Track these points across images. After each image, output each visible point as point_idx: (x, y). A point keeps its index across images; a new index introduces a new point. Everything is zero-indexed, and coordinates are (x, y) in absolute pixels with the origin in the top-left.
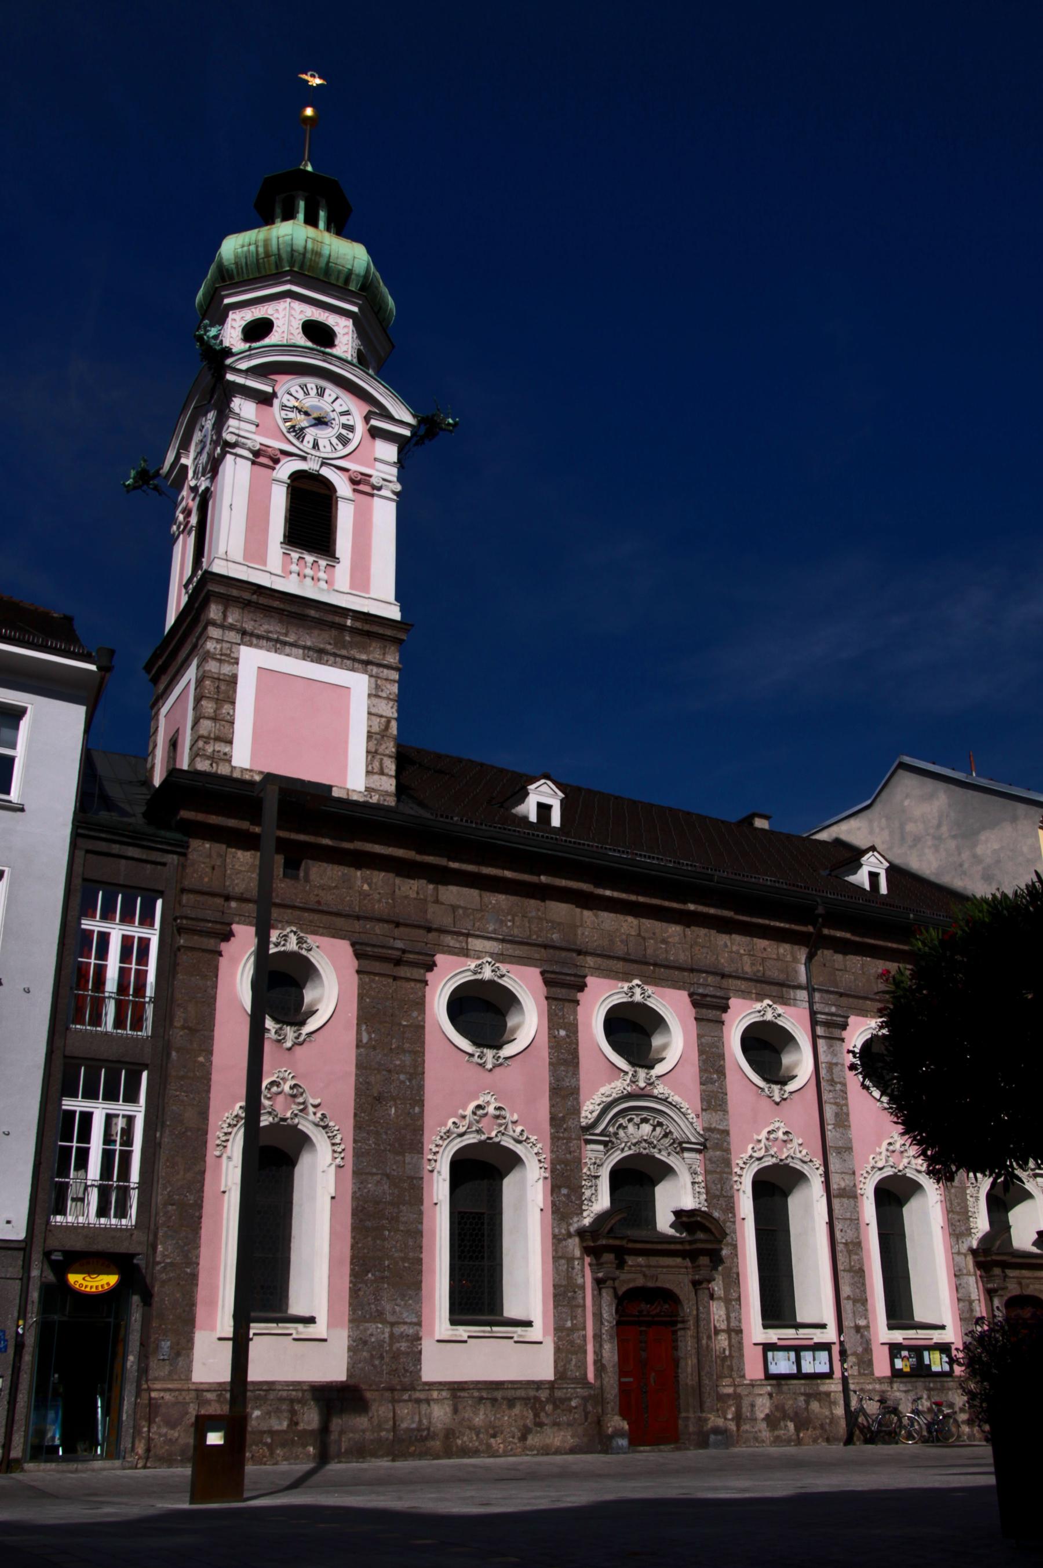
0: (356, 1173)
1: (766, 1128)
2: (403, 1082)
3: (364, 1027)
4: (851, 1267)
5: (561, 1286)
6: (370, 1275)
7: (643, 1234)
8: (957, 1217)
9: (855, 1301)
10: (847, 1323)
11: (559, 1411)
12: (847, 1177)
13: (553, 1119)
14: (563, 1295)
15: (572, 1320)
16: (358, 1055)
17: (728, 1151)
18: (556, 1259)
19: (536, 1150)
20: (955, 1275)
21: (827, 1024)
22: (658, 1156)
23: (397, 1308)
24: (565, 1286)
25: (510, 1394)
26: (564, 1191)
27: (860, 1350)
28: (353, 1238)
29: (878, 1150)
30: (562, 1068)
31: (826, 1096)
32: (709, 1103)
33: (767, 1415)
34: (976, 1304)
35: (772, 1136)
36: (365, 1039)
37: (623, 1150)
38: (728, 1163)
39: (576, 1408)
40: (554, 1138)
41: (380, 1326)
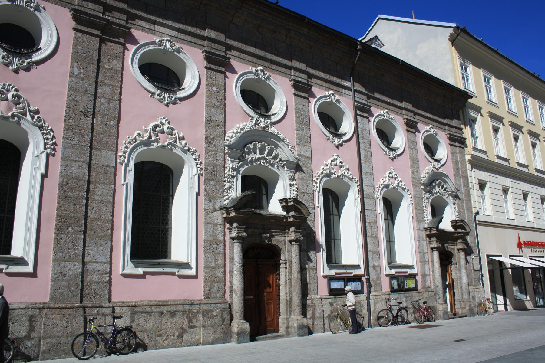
2: (103, 104)
3: (75, 64)
4: (372, 235)
5: (208, 241)
6: (70, 229)
7: (262, 212)
8: (419, 212)
9: (373, 253)
11: (205, 318)
12: (370, 188)
13: (206, 138)
14: (210, 246)
15: (215, 262)
16: (71, 82)
19: (194, 156)
23: (91, 252)
24: (211, 241)
25: (173, 308)
26: (212, 183)
28: (58, 203)
30: (214, 109)
31: (361, 145)
32: (300, 140)
33: (329, 315)
34: (426, 255)
35: (333, 163)
36: (76, 72)
39: (216, 316)
41: (77, 264)
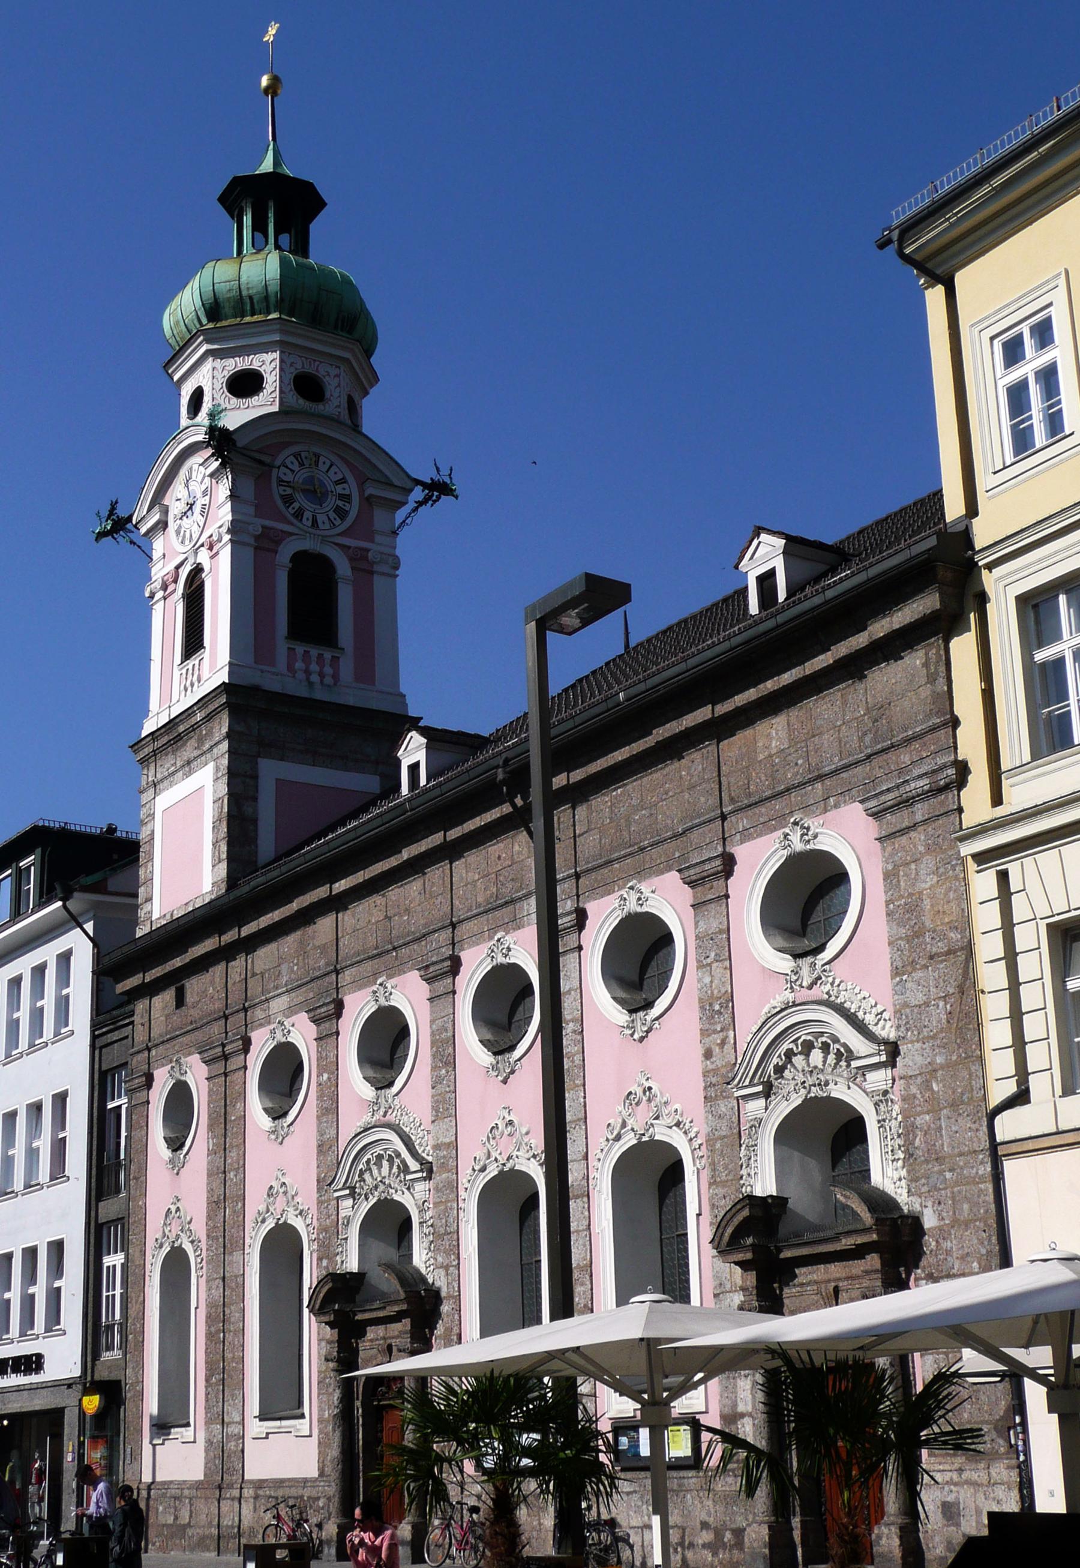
8: (721, 1191)
13: (318, 1181)
22: (396, 1197)
32: (437, 1111)
37: (367, 1199)
40: (320, 1202)
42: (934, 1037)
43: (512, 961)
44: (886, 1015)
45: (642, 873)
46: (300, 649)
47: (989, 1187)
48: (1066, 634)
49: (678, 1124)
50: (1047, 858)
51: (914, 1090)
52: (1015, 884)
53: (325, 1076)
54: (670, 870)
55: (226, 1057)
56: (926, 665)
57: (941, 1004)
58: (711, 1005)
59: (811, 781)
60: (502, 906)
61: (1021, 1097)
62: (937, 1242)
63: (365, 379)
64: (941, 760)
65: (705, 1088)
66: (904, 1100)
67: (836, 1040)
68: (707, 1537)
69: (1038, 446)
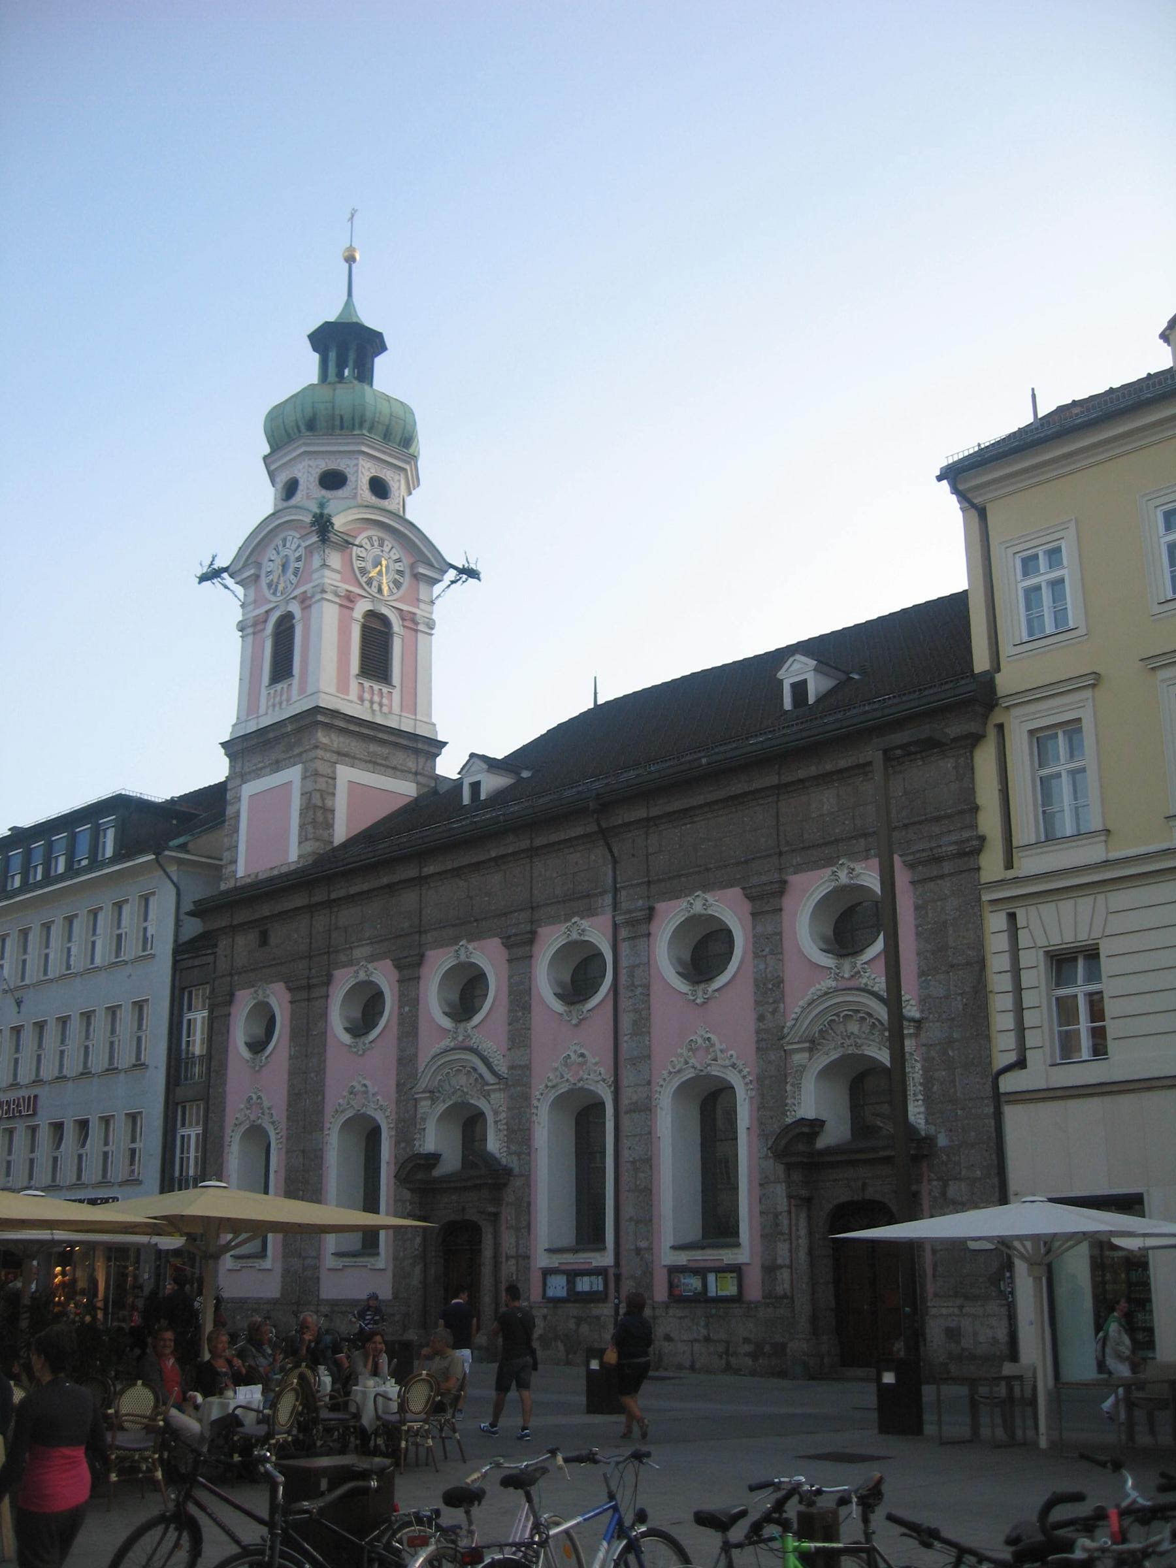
0: (287, 1152)
1: (571, 1050)
10: (627, 1245)
13: (399, 1085)
17: (528, 1085)
18: (396, 1201)
20: (761, 1185)
21: (632, 923)
22: (472, 1101)
27: (638, 1273)
29: (679, 1051)
37: (444, 1101)
38: (526, 1097)
40: (398, 1101)
42: (953, 1019)
43: (586, 938)
44: (913, 1002)
45: (707, 887)
46: (367, 684)
47: (992, 1122)
48: (1062, 761)
49: (734, 1066)
50: (1048, 910)
51: (933, 1053)
52: (1021, 921)
53: (407, 1009)
54: (731, 885)
55: (309, 987)
56: (956, 768)
57: (959, 998)
58: (765, 984)
59: (855, 837)
60: (579, 899)
61: (1021, 1064)
62: (948, 1156)
63: (413, 483)
64: (966, 834)
65: (758, 1042)
66: (925, 1060)
67: (870, 1015)
68: (748, 1348)
69: (1048, 631)
